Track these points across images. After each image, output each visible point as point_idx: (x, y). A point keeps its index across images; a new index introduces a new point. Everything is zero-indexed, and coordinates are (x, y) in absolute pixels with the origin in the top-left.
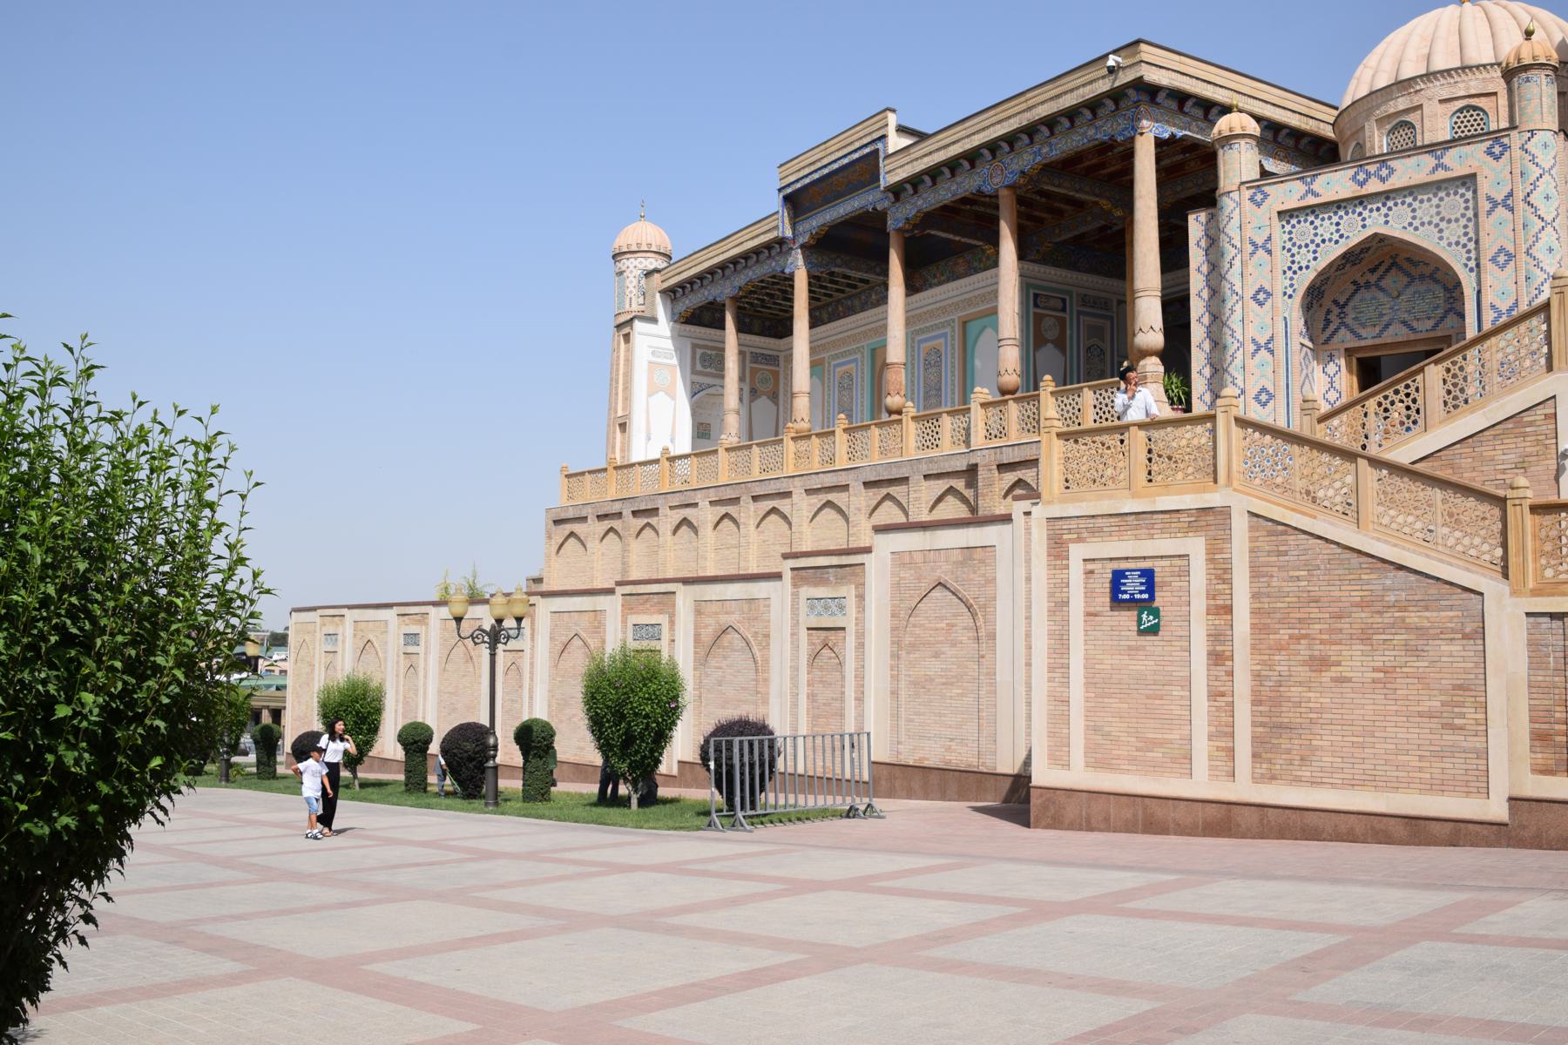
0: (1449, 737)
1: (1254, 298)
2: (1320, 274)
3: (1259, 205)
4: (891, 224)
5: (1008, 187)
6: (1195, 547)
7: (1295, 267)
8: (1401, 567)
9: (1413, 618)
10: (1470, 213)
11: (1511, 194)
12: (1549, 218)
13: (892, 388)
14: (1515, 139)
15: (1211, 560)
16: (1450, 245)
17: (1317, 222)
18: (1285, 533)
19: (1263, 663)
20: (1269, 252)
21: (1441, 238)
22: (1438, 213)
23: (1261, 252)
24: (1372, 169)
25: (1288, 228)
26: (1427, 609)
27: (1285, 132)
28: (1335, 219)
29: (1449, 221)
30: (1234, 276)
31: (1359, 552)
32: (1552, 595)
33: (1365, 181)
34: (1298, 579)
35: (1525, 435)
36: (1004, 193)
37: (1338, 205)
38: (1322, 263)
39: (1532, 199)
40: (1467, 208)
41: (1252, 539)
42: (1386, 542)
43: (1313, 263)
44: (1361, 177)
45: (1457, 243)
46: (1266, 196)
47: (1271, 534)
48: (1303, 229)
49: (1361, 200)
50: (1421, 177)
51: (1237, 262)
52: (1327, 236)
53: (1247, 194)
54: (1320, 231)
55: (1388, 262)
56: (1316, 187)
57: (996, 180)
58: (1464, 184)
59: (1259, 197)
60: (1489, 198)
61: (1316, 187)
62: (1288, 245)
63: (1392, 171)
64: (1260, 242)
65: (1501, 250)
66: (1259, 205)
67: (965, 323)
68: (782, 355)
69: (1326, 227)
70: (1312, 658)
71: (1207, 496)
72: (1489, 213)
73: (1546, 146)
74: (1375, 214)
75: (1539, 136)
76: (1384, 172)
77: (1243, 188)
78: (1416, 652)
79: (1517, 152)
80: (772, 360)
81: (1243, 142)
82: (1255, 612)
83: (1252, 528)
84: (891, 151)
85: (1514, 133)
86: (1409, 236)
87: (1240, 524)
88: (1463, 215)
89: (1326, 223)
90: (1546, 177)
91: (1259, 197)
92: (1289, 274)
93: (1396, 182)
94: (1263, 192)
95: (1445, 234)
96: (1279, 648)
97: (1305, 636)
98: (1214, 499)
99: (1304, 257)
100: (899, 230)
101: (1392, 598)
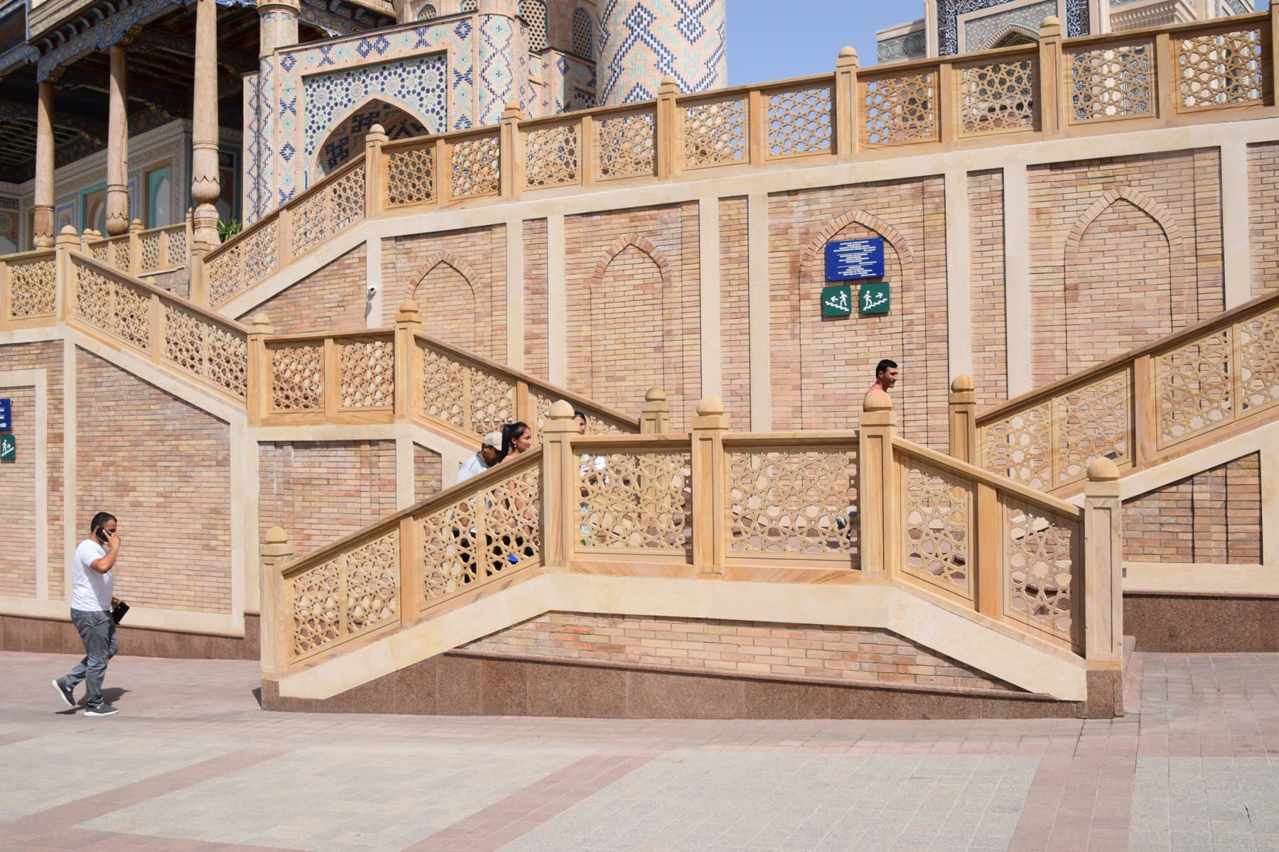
0: (208, 558)
1: (282, 153)
2: (334, 134)
3: (288, 69)
4: (42, 76)
5: (116, 45)
6: (39, 377)
7: (315, 127)
8: (177, 399)
9: (185, 446)
10: (443, 85)
11: (470, 70)
12: (499, 92)
13: (37, 228)
14: (476, 21)
15: (51, 391)
16: (427, 111)
17: (332, 87)
18: (100, 366)
19: (85, 488)
20: (294, 112)
21: (421, 106)
22: (420, 84)
23: (288, 111)
24: (372, 41)
25: (310, 91)
26: (193, 437)
27: (360, 12)
28: (345, 85)
29: (428, 91)
30: (267, 133)
31: (150, 384)
32: (275, 425)
33: (368, 51)
34: (108, 409)
35: (345, 276)
36: (113, 50)
37: (347, 72)
38: (334, 125)
39: (486, 74)
40: (441, 80)
41: (79, 371)
42: (166, 374)
43: (327, 124)
44: (364, 48)
45: (433, 111)
46: (294, 61)
47: (92, 366)
48: (322, 92)
49: (365, 69)
50: (408, 51)
51: (270, 120)
52: (339, 100)
53: (281, 58)
54: (334, 95)
55: (399, 126)
56: (331, 55)
57: (108, 38)
58: (440, 59)
59: (288, 62)
60: (456, 72)
61: (331, 55)
62: (310, 107)
63: (387, 44)
64: (288, 103)
65: (463, 118)
66: (288, 69)
67: (147, 174)
68: (21, 199)
69: (338, 92)
70: (118, 484)
71: (48, 329)
72: (456, 85)
73: (499, 29)
74: (374, 81)
75: (495, 21)
76: (381, 45)
77: (277, 53)
78: (185, 478)
79: (475, 32)
80: (13, 203)
81: (279, 12)
82: (80, 440)
83: (79, 361)
84: (34, 5)
85: (475, 16)
86: (398, 103)
87: (70, 355)
88: (438, 86)
89: (339, 88)
90: (498, 56)
91: (288, 62)
92: (310, 132)
93: (390, 54)
94: (291, 58)
95: (424, 102)
96: (96, 475)
97: (113, 464)
98: (52, 333)
99: (321, 118)
100: (45, 82)
101: (171, 427)
